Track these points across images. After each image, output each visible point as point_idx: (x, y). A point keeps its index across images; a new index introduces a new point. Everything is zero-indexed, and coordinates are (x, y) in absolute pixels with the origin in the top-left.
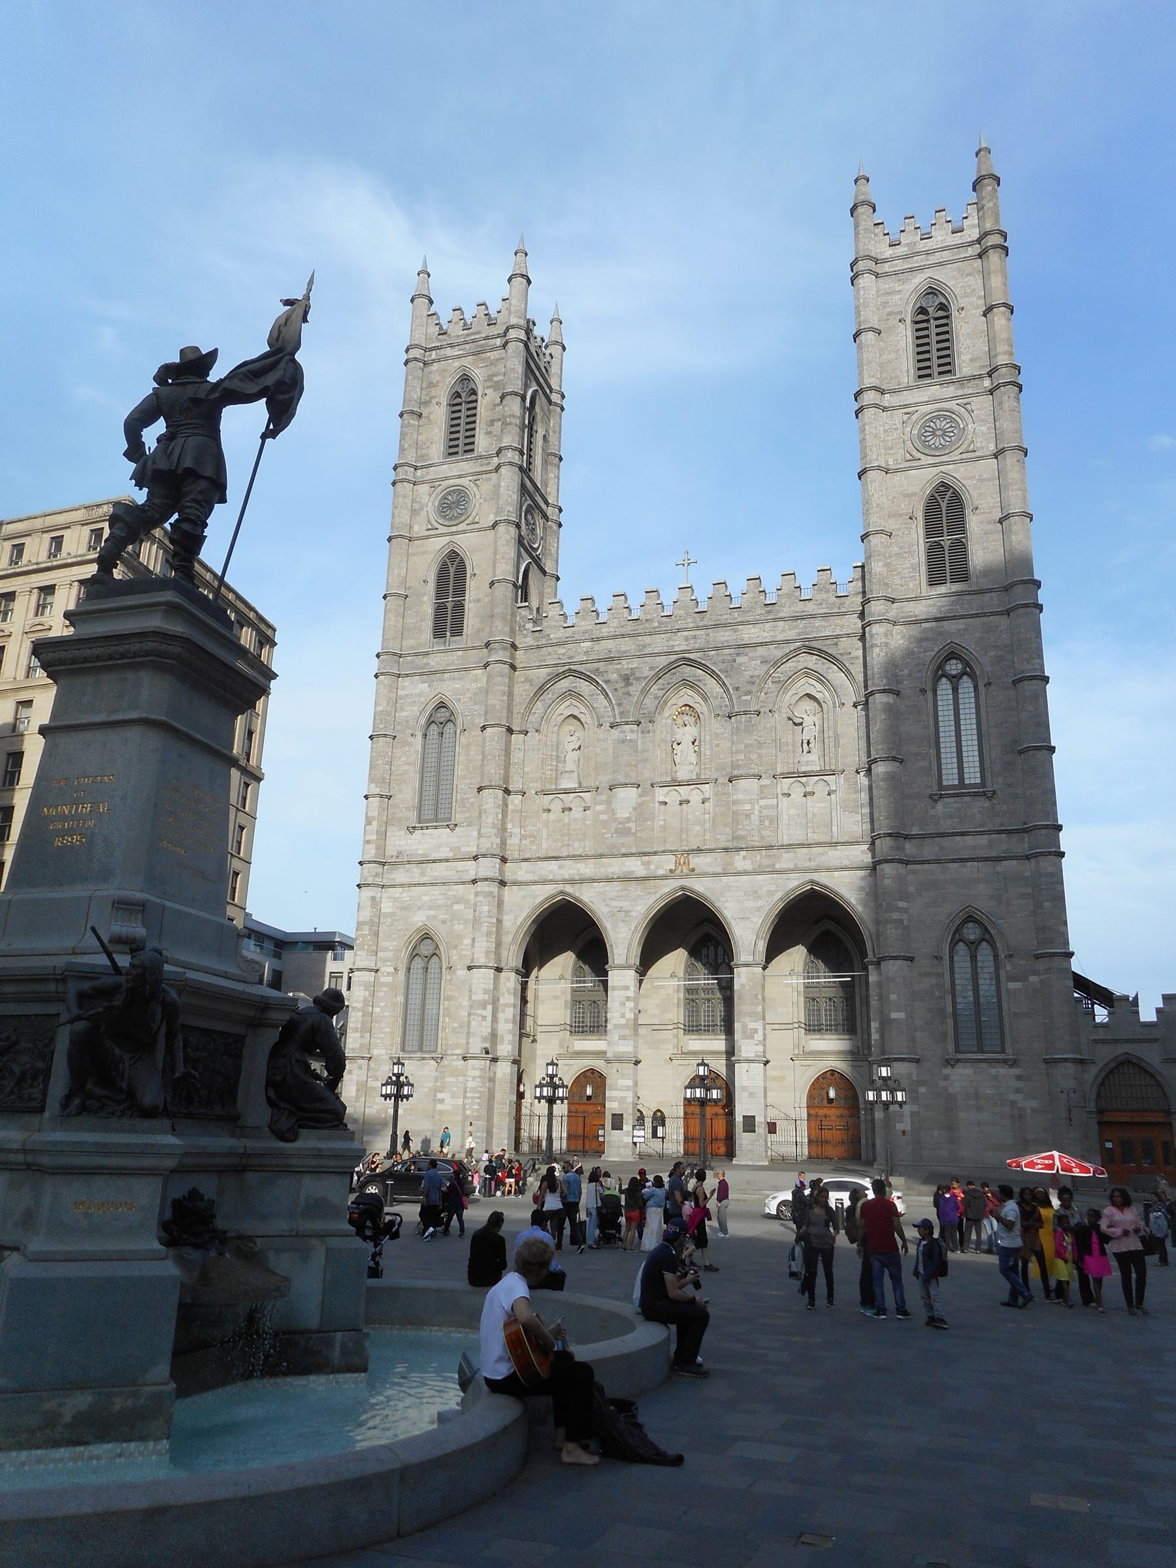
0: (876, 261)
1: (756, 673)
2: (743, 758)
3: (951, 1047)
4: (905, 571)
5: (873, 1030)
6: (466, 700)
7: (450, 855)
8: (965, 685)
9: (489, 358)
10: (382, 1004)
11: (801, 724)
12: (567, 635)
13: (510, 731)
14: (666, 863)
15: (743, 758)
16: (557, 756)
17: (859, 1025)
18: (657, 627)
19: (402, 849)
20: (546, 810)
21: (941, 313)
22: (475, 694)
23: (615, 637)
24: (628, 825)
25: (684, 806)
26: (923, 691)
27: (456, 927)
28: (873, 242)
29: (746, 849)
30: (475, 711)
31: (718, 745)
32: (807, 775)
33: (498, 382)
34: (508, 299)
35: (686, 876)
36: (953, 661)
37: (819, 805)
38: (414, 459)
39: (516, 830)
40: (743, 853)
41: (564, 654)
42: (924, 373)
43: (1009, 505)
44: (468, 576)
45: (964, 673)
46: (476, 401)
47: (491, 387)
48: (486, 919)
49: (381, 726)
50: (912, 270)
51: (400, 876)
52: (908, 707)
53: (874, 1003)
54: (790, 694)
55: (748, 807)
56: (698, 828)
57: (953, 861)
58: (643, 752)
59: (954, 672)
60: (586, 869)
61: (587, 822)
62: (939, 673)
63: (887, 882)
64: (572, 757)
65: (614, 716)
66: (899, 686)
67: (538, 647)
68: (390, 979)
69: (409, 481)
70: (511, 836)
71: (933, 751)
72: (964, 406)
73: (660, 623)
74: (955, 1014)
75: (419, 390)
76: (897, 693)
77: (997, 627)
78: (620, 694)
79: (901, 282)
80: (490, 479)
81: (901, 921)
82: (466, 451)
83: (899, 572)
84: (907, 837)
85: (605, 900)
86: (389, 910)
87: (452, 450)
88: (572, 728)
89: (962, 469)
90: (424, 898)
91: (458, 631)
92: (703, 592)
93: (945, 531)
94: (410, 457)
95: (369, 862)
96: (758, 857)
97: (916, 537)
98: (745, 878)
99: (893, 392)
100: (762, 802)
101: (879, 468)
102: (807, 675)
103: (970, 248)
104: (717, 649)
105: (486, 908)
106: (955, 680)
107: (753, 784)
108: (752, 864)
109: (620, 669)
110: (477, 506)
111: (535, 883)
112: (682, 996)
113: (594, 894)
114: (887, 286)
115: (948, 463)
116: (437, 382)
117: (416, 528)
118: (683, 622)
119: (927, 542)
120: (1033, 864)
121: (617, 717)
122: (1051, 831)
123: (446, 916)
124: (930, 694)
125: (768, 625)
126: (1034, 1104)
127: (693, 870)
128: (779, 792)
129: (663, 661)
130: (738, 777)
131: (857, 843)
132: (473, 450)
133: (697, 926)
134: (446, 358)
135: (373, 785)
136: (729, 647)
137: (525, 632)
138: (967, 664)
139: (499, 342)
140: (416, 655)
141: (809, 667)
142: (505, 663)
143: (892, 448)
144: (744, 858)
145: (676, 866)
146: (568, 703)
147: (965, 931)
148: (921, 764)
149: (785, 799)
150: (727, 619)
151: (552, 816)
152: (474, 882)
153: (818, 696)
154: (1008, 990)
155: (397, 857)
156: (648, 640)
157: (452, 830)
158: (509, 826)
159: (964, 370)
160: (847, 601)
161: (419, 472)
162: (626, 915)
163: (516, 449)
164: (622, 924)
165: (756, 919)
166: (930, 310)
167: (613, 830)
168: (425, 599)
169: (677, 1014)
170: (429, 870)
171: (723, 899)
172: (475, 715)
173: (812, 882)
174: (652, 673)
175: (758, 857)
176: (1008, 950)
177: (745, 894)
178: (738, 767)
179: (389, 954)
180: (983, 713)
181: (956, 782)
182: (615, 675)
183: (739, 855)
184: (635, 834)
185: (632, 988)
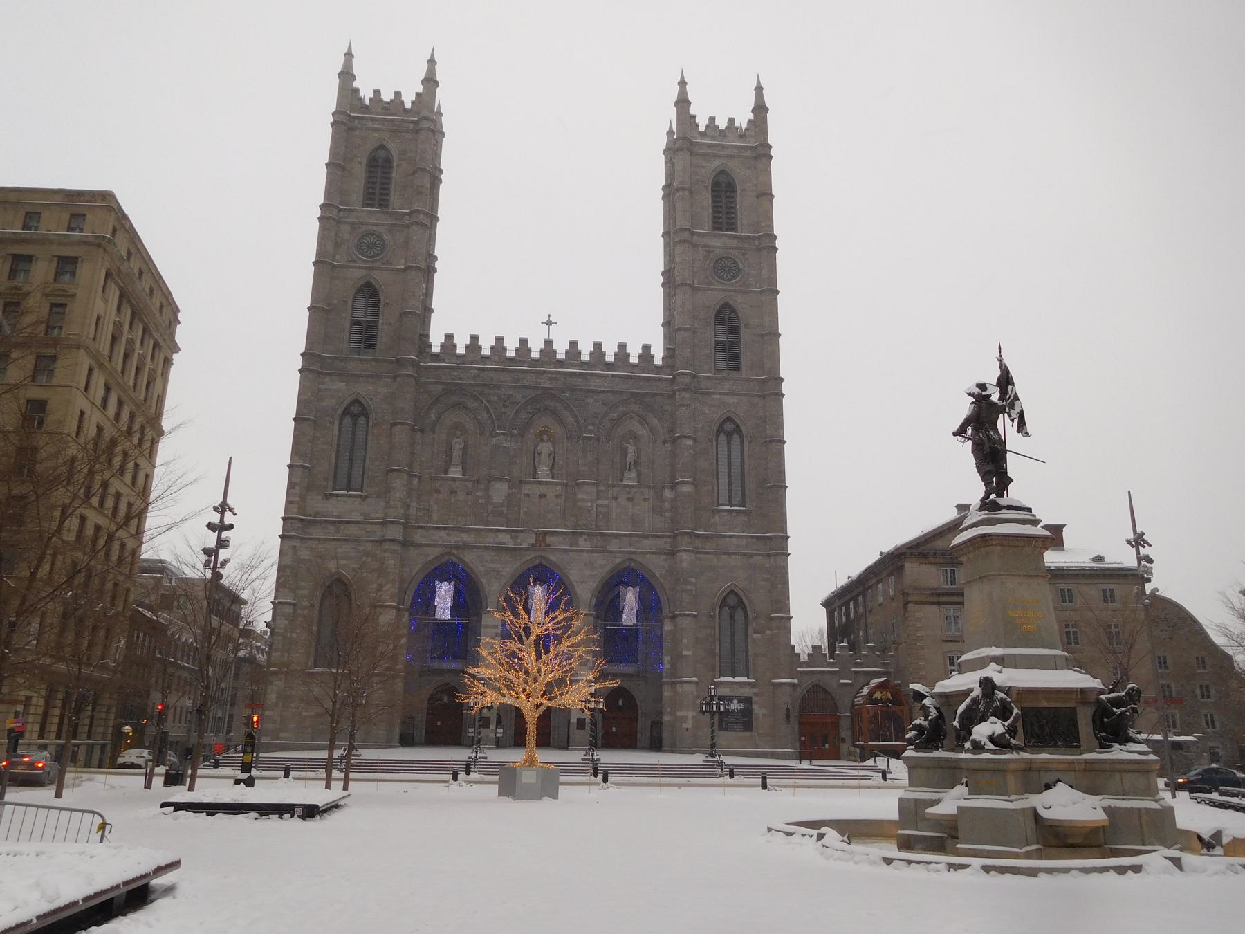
0: (692, 144)
3: (717, 674)
5: (666, 662)
6: (377, 400)
11: (627, 450)
13: (413, 430)
16: (446, 451)
24: (501, 509)
25: (543, 500)
26: (711, 441)
35: (543, 550)
36: (729, 423)
40: (585, 537)
41: (456, 376)
42: (717, 225)
46: (391, 167)
49: (306, 411)
50: (715, 156)
51: (317, 532)
53: (667, 644)
55: (590, 504)
57: (725, 554)
60: (468, 539)
61: (469, 503)
62: (720, 430)
64: (457, 454)
69: (334, 219)
70: (409, 507)
71: (715, 480)
72: (744, 254)
74: (720, 655)
76: (695, 440)
82: (380, 206)
85: (482, 562)
86: (307, 558)
87: (369, 200)
90: (340, 550)
91: (373, 346)
92: (561, 351)
95: (293, 518)
96: (595, 540)
100: (599, 502)
101: (689, 285)
102: (631, 418)
104: (572, 390)
105: (392, 562)
106: (729, 435)
107: (593, 489)
110: (391, 250)
111: (427, 545)
115: (732, 291)
119: (716, 341)
120: (772, 561)
123: (357, 566)
124: (714, 444)
126: (764, 711)
127: (549, 545)
128: (610, 495)
135: (296, 458)
136: (581, 390)
139: (411, 126)
143: (696, 273)
144: (585, 540)
145: (536, 541)
147: (728, 599)
152: (381, 541)
154: (753, 638)
157: (363, 500)
161: (341, 214)
163: (426, 214)
166: (723, 185)
167: (489, 511)
168: (344, 315)
170: (342, 528)
173: (631, 559)
175: (595, 540)
179: (306, 592)
182: (496, 398)
183: (582, 537)
185: (500, 627)
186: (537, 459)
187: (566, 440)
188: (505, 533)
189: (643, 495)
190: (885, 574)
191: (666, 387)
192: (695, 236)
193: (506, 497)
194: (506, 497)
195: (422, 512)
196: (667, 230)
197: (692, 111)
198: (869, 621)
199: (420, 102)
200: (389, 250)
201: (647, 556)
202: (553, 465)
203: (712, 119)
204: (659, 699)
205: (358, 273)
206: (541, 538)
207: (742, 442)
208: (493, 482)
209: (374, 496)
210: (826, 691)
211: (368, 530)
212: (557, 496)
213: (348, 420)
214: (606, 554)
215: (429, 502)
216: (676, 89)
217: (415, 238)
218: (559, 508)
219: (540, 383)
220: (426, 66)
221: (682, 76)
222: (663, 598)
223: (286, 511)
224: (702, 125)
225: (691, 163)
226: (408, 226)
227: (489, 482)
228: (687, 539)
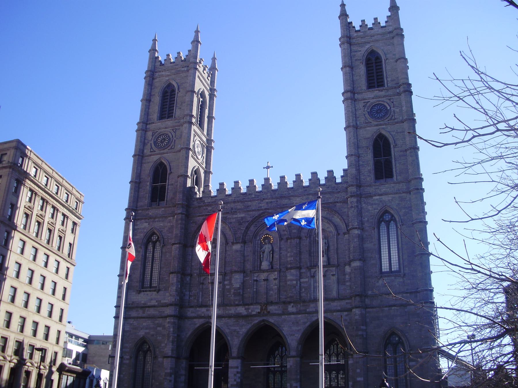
2: (293, 259)
4: (365, 173)
6: (165, 231)
7: (156, 304)
8: (392, 225)
10: (124, 373)
12: (213, 201)
14: (256, 309)
15: (293, 259)
18: (254, 198)
19: (134, 300)
20: (201, 283)
23: (234, 202)
24: (239, 291)
27: (158, 338)
28: (348, 30)
29: (294, 302)
30: (169, 236)
31: (282, 253)
36: (387, 214)
37: (328, 281)
38: (146, 120)
39: (188, 293)
40: (292, 304)
41: (211, 210)
44: (168, 173)
46: (175, 94)
48: (172, 335)
52: (367, 235)
55: (295, 282)
56: (272, 292)
57: (386, 307)
58: (248, 256)
59: (387, 219)
66: (364, 226)
67: (199, 207)
68: (127, 362)
70: (185, 296)
73: (255, 195)
75: (150, 90)
76: (362, 229)
77: (405, 198)
79: (361, 47)
81: (362, 335)
82: (169, 117)
84: (366, 296)
86: (128, 329)
87: (162, 117)
89: (389, 128)
91: (162, 198)
93: (382, 155)
97: (369, 157)
98: (293, 316)
99: (358, 93)
100: (302, 280)
103: (388, 35)
105: (172, 329)
108: (296, 309)
109: (236, 218)
110: (173, 141)
113: (222, 323)
114: (355, 48)
117: (145, 151)
122: (429, 292)
123: (154, 333)
124: (376, 230)
125: (304, 197)
127: (269, 312)
129: (256, 214)
130: (291, 268)
134: (162, 76)
137: (193, 200)
138: (392, 216)
139: (185, 69)
140: (143, 210)
142: (184, 214)
143: (358, 118)
144: (293, 307)
145: (261, 310)
148: (373, 262)
149: (312, 280)
150: (286, 194)
151: (204, 287)
155: (132, 304)
156: (250, 203)
158: (184, 291)
159: (389, 85)
161: (148, 126)
164: (235, 337)
165: (297, 335)
171: (282, 326)
174: (251, 219)
175: (299, 306)
176: (410, 348)
177: (293, 323)
178: (291, 264)
180: (400, 238)
181: (388, 270)
183: (290, 305)
185: (240, 368)
186: (262, 256)
187: (279, 242)
188: (241, 307)
191: (344, 197)
193: (242, 283)
194: (242, 283)
195: (193, 297)
197: (349, 20)
199: (190, 55)
200: (172, 141)
201: (334, 314)
205: (155, 158)
206: (264, 308)
208: (234, 274)
209: (163, 290)
211: (160, 311)
212: (275, 279)
214: (307, 315)
215: (196, 291)
216: (339, 9)
217: (185, 131)
218: (276, 287)
219: (261, 207)
220: (194, 34)
221: (343, 1)
224: (357, 25)
225: (351, 50)
228: (358, 299)
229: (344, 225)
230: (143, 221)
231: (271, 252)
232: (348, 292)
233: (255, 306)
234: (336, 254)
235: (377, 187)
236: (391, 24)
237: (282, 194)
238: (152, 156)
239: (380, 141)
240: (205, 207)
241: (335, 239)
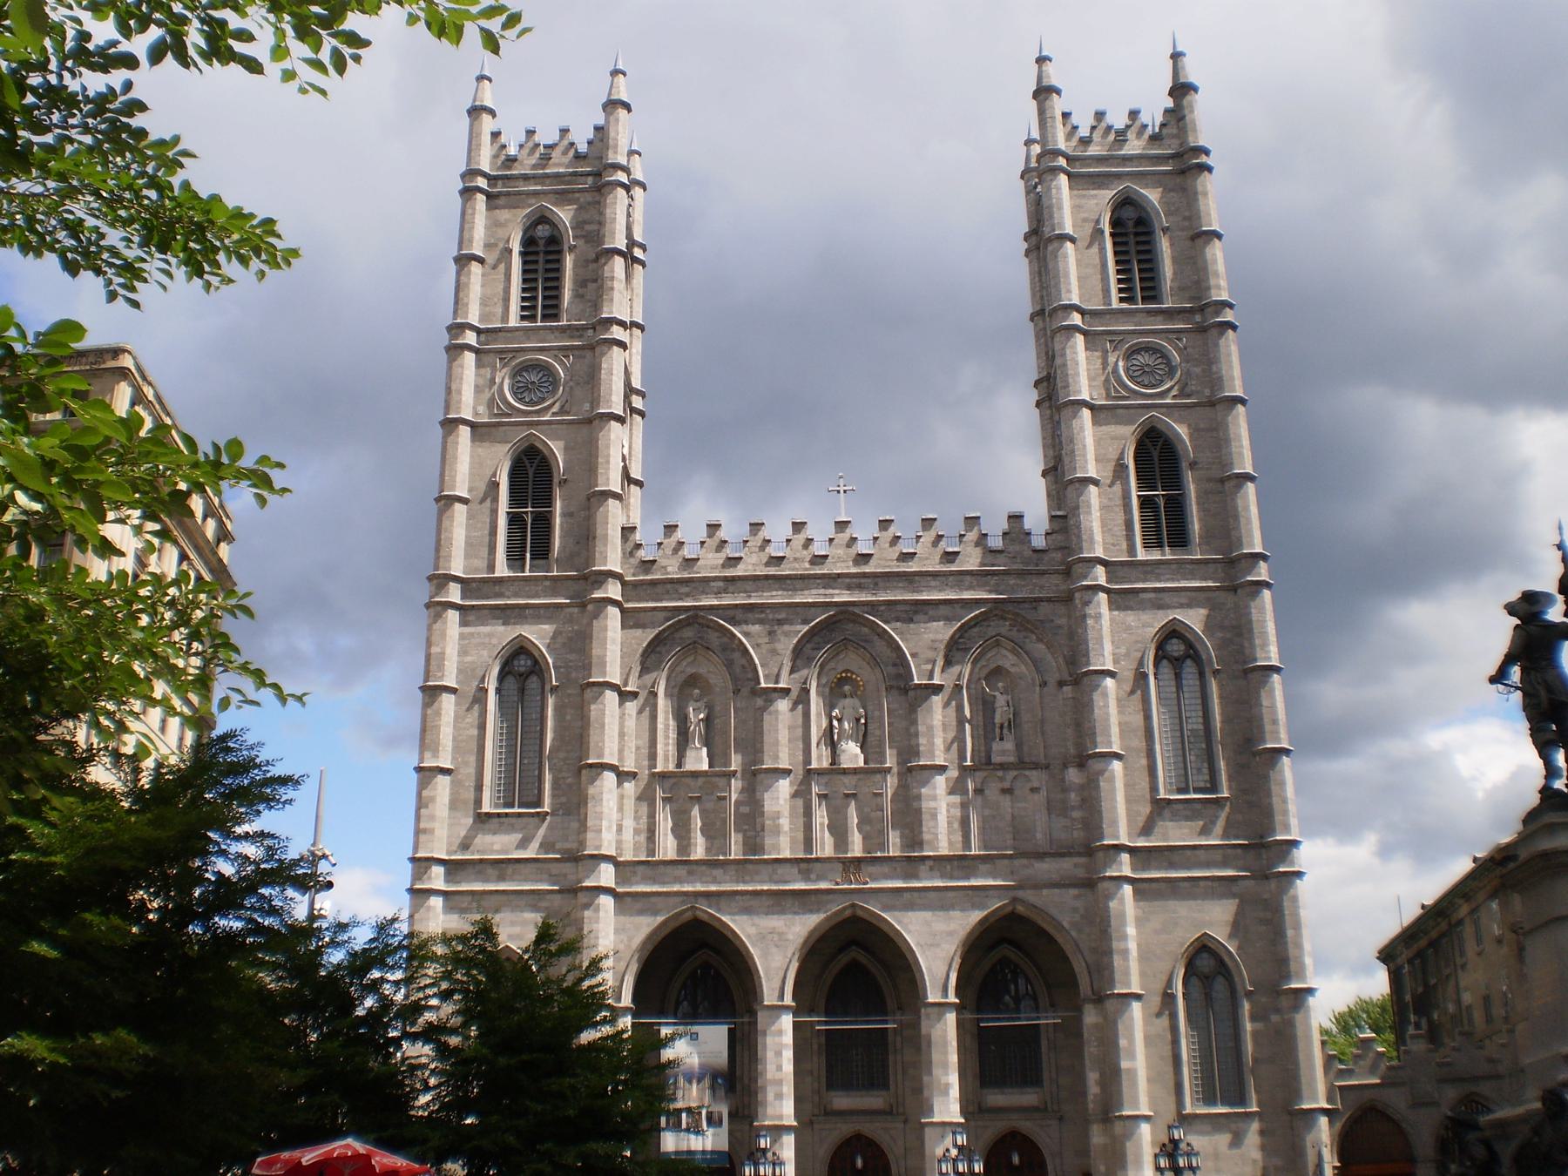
1: (940, 637)
4: (1116, 529)
9: (578, 199)
17: (1046, 1075)
21: (1140, 229)
22: (571, 639)
30: (571, 661)
32: (1003, 767)
33: (590, 232)
34: (602, 128)
36: (1174, 641)
37: (1019, 805)
39: (629, 824)
43: (1232, 463)
44: (556, 481)
45: (1189, 656)
47: (583, 237)
53: (1091, 1050)
54: (979, 666)
55: (932, 804)
56: (868, 828)
59: (1176, 654)
63: (1113, 904)
65: (759, 683)
70: (620, 829)
77: (1223, 604)
78: (764, 651)
80: (585, 357)
83: (1110, 529)
88: (697, 691)
94: (470, 315)
96: (948, 867)
102: (998, 644)
112: (823, 1040)
116: (507, 221)
118: (843, 565)
119: (1139, 496)
121: (762, 680)
125: (951, 578)
131: (1070, 855)
132: (556, 317)
133: (841, 950)
134: (519, 193)
139: (590, 180)
141: (1003, 631)
144: (931, 869)
146: (692, 658)
147: (1198, 963)
153: (1012, 670)
160: (1046, 558)
161: (483, 337)
162: (780, 940)
164: (774, 950)
169: (818, 1063)
170: (510, 871)
172: (571, 667)
175: (948, 867)
183: (924, 864)
184: (786, 832)
187: (884, 694)
188: (788, 865)
189: (1029, 780)
190: (1481, 896)
191: (1057, 585)
192: (1086, 316)
193: (785, 800)
196: (1038, 308)
198: (1462, 984)
199: (602, 140)
201: (1045, 892)
202: (865, 735)
203: (1100, 115)
204: (1084, 1151)
207: (1202, 675)
208: (763, 775)
209: (561, 812)
210: (1389, 1119)
213: (511, 682)
217: (604, 366)
219: (832, 595)
222: (1079, 966)
223: (416, 848)
226: (592, 348)
227: (755, 775)
229: (1061, 660)
230: (486, 612)
231: (863, 721)
232: (1076, 834)
233: (827, 866)
234: (1039, 735)
235: (1149, 569)
236: (1175, 131)
237: (889, 566)
238: (504, 428)
239: (1152, 448)
240: (669, 586)
241: (1037, 696)
